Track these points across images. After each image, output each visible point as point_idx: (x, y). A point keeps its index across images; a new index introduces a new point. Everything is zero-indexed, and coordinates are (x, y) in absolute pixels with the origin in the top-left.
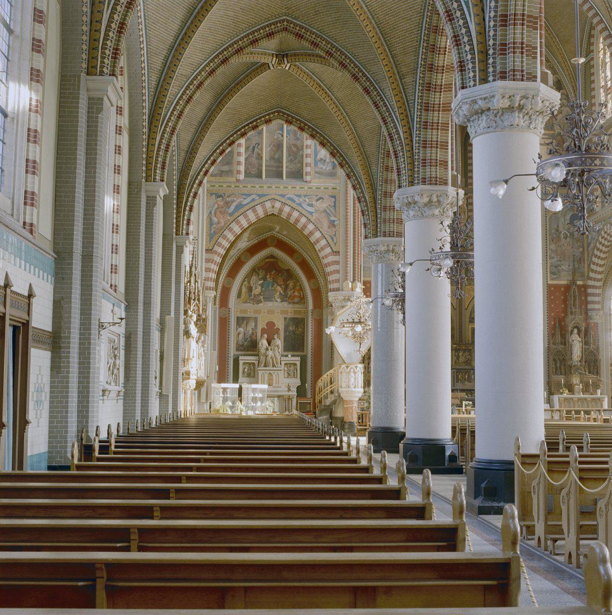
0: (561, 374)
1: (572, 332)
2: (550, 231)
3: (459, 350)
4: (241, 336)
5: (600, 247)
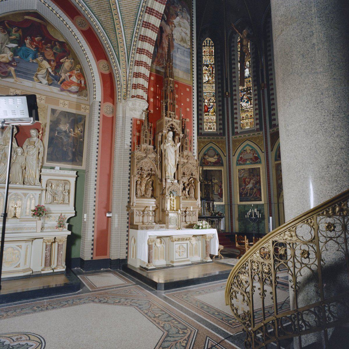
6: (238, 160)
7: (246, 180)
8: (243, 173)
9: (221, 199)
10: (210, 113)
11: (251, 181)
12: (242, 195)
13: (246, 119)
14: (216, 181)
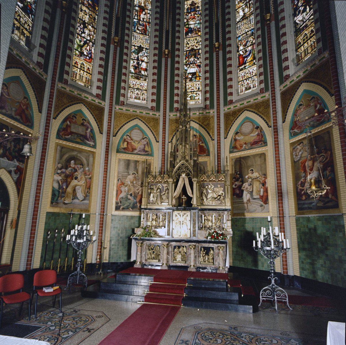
6: (292, 128)
7: (306, 164)
8: (300, 151)
9: (266, 206)
10: (247, 64)
11: (315, 164)
12: (302, 196)
13: (304, 43)
14: (256, 175)
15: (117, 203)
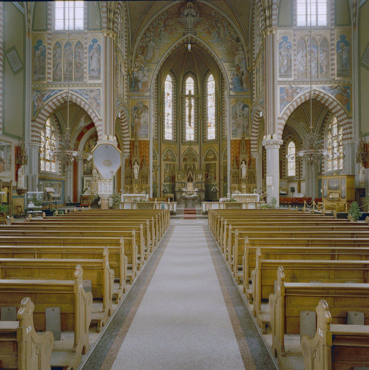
0: (237, 183)
1: (242, 163)
2: (232, 113)
3: (198, 173)
4: (86, 168)
5: (255, 119)
6: (224, 157)
14: (213, 170)
15: (164, 180)
